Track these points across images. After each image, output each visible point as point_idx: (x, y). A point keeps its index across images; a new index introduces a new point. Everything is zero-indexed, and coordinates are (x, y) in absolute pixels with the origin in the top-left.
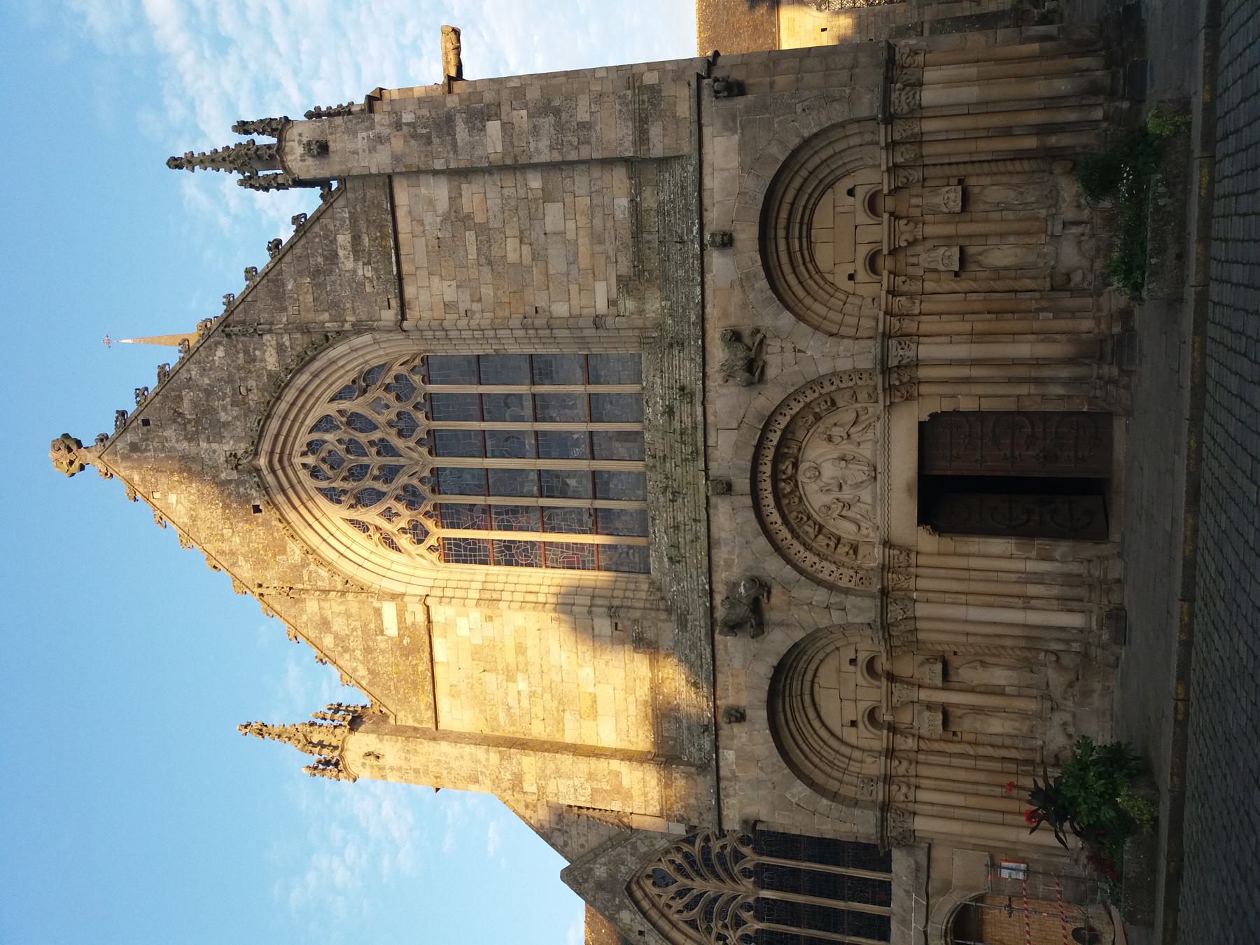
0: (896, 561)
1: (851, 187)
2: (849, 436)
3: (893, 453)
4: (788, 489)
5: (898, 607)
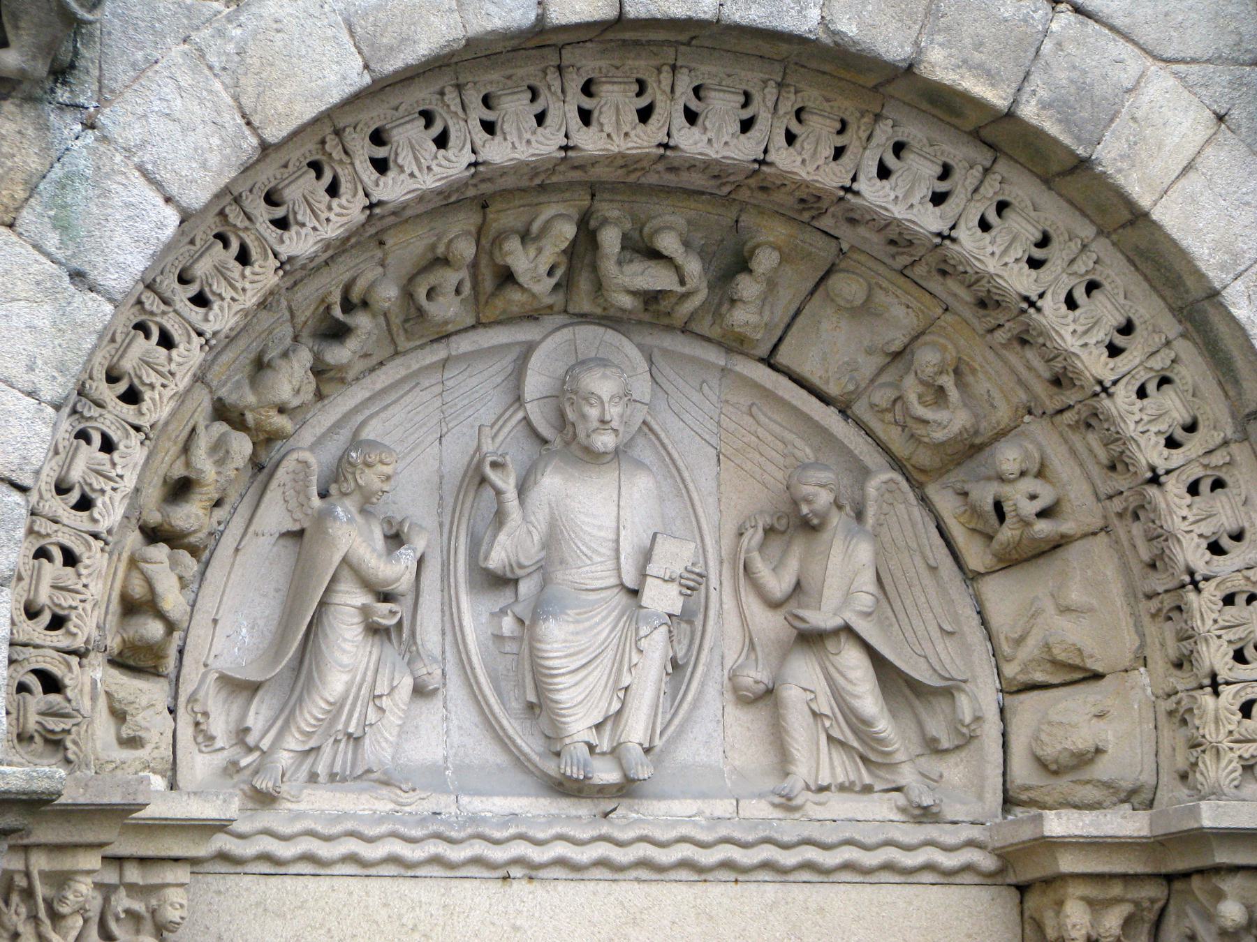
2: (811, 639)
3: (719, 894)
4: (520, 260)
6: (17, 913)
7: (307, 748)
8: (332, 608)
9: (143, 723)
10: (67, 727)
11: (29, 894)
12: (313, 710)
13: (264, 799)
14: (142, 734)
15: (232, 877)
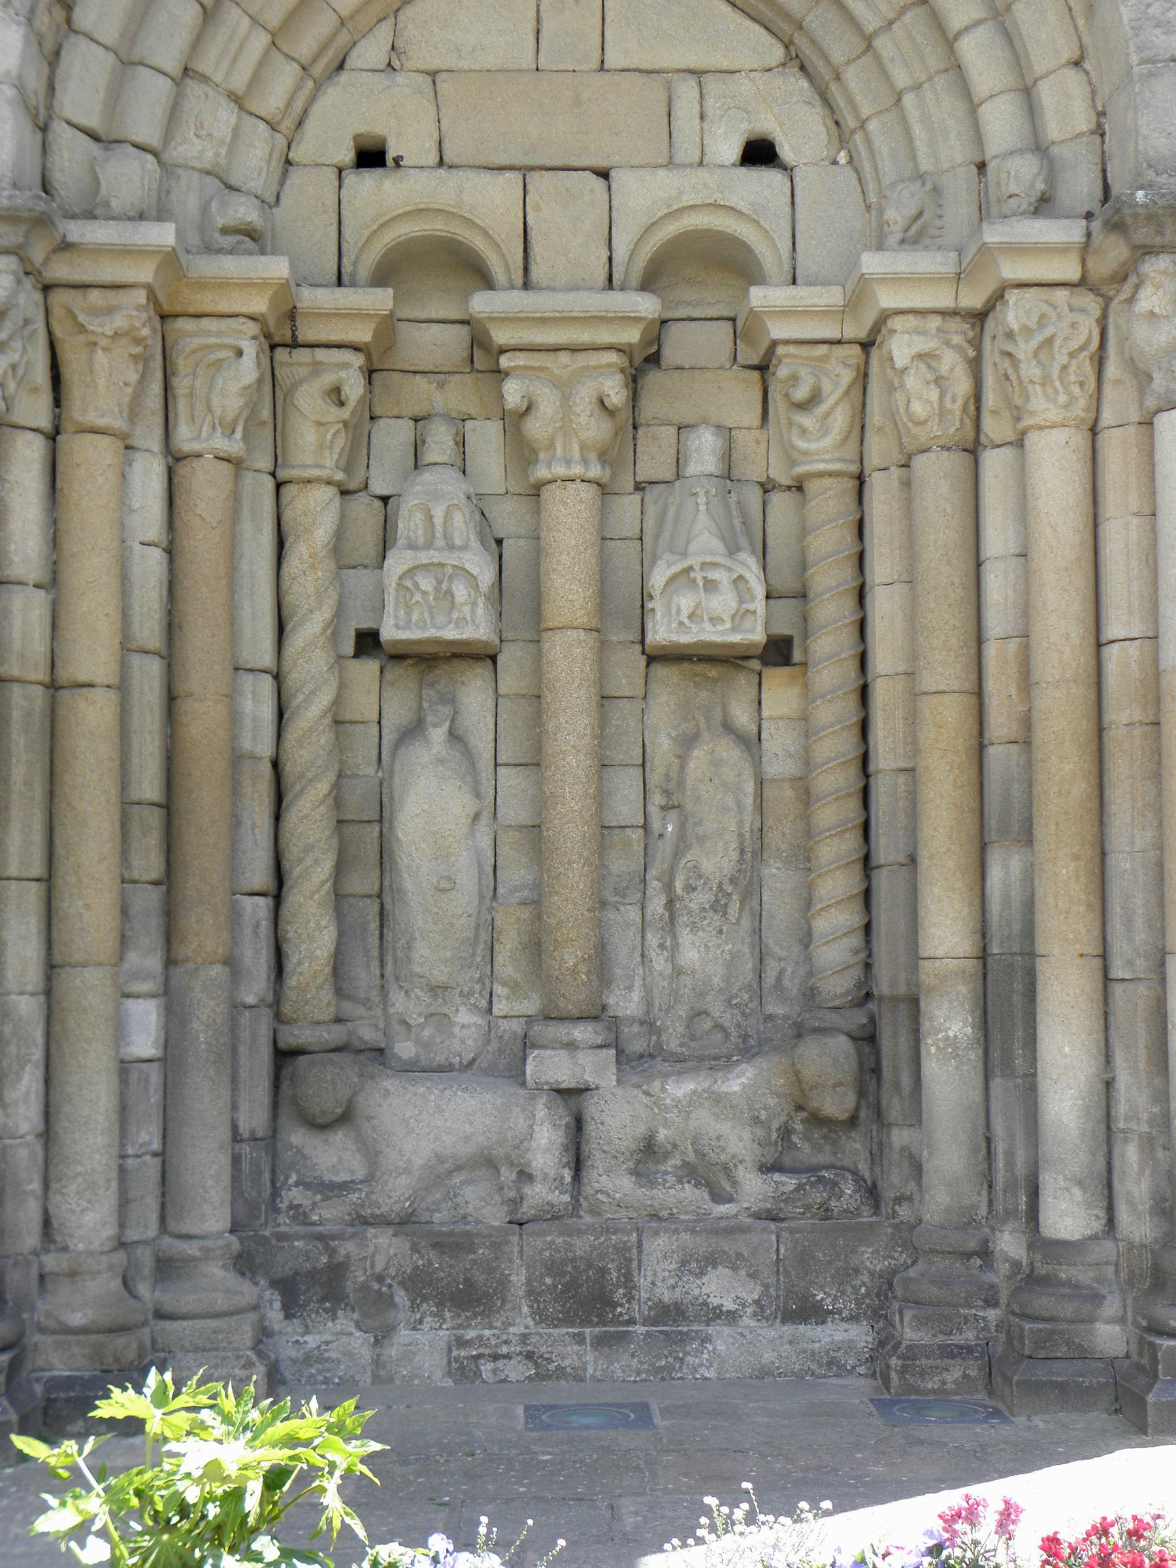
1: (785, 152)
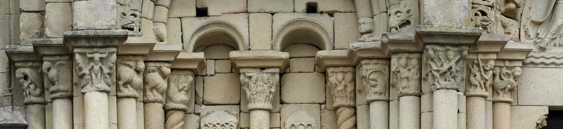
0: (505, 70)
5: (453, 63)
6: (475, 70)
7: (553, 38)
8: (558, 5)
9: (510, 29)
10: (488, 24)
11: (478, 65)
12: (554, 28)
13: (543, 49)
14: (510, 31)
15: (535, 68)
